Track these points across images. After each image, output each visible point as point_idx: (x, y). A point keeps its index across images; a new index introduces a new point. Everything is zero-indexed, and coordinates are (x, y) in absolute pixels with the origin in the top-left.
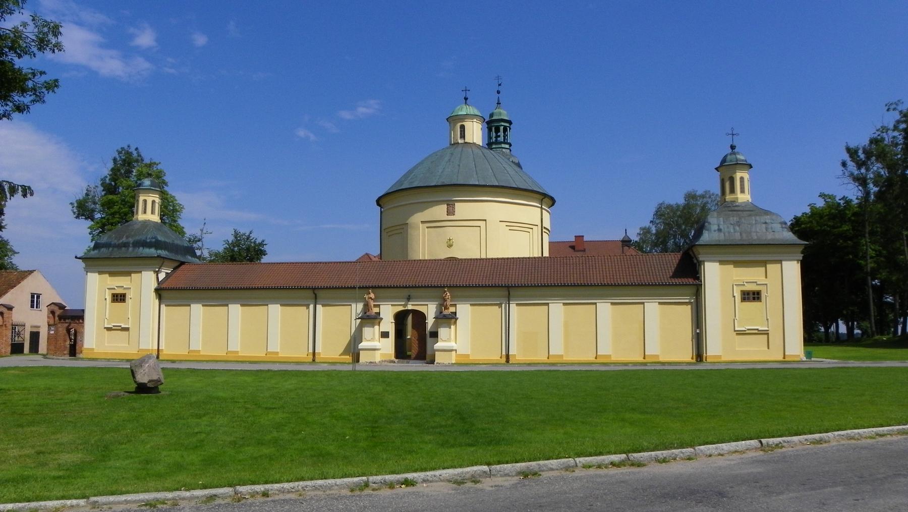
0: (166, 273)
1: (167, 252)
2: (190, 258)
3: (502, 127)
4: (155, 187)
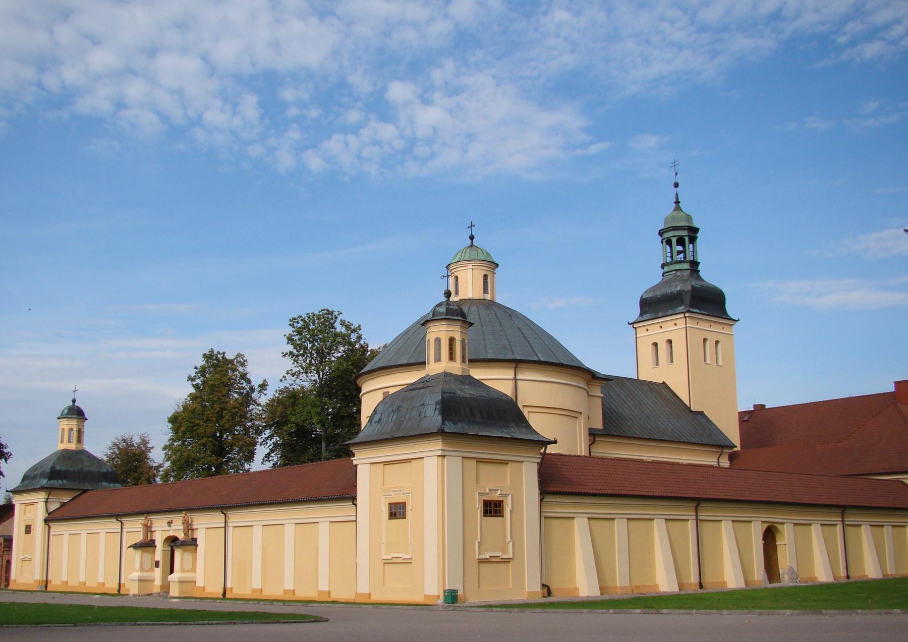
0: (61, 503)
1: (65, 482)
2: (105, 484)
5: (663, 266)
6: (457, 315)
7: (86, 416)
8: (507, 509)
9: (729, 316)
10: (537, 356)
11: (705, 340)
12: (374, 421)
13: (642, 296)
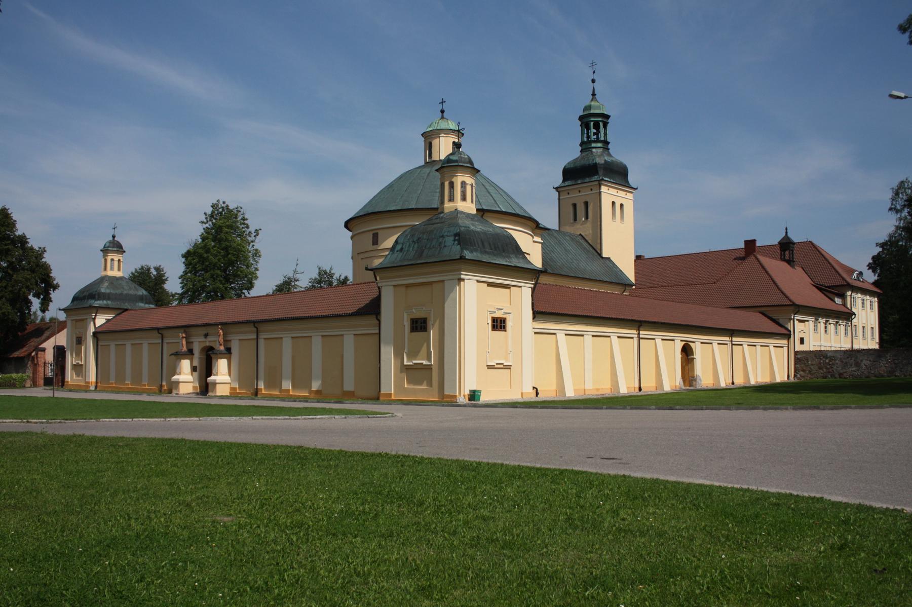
1: (109, 302)
3: (592, 123)
4: (113, 247)
5: (581, 145)
6: (467, 163)
7: (124, 249)
8: (509, 324)
9: (629, 184)
10: (499, 207)
11: (613, 203)
12: (396, 250)
13: (565, 167)
